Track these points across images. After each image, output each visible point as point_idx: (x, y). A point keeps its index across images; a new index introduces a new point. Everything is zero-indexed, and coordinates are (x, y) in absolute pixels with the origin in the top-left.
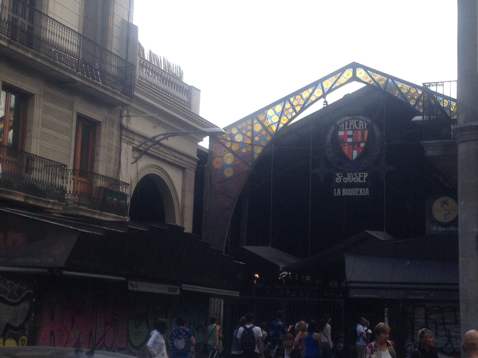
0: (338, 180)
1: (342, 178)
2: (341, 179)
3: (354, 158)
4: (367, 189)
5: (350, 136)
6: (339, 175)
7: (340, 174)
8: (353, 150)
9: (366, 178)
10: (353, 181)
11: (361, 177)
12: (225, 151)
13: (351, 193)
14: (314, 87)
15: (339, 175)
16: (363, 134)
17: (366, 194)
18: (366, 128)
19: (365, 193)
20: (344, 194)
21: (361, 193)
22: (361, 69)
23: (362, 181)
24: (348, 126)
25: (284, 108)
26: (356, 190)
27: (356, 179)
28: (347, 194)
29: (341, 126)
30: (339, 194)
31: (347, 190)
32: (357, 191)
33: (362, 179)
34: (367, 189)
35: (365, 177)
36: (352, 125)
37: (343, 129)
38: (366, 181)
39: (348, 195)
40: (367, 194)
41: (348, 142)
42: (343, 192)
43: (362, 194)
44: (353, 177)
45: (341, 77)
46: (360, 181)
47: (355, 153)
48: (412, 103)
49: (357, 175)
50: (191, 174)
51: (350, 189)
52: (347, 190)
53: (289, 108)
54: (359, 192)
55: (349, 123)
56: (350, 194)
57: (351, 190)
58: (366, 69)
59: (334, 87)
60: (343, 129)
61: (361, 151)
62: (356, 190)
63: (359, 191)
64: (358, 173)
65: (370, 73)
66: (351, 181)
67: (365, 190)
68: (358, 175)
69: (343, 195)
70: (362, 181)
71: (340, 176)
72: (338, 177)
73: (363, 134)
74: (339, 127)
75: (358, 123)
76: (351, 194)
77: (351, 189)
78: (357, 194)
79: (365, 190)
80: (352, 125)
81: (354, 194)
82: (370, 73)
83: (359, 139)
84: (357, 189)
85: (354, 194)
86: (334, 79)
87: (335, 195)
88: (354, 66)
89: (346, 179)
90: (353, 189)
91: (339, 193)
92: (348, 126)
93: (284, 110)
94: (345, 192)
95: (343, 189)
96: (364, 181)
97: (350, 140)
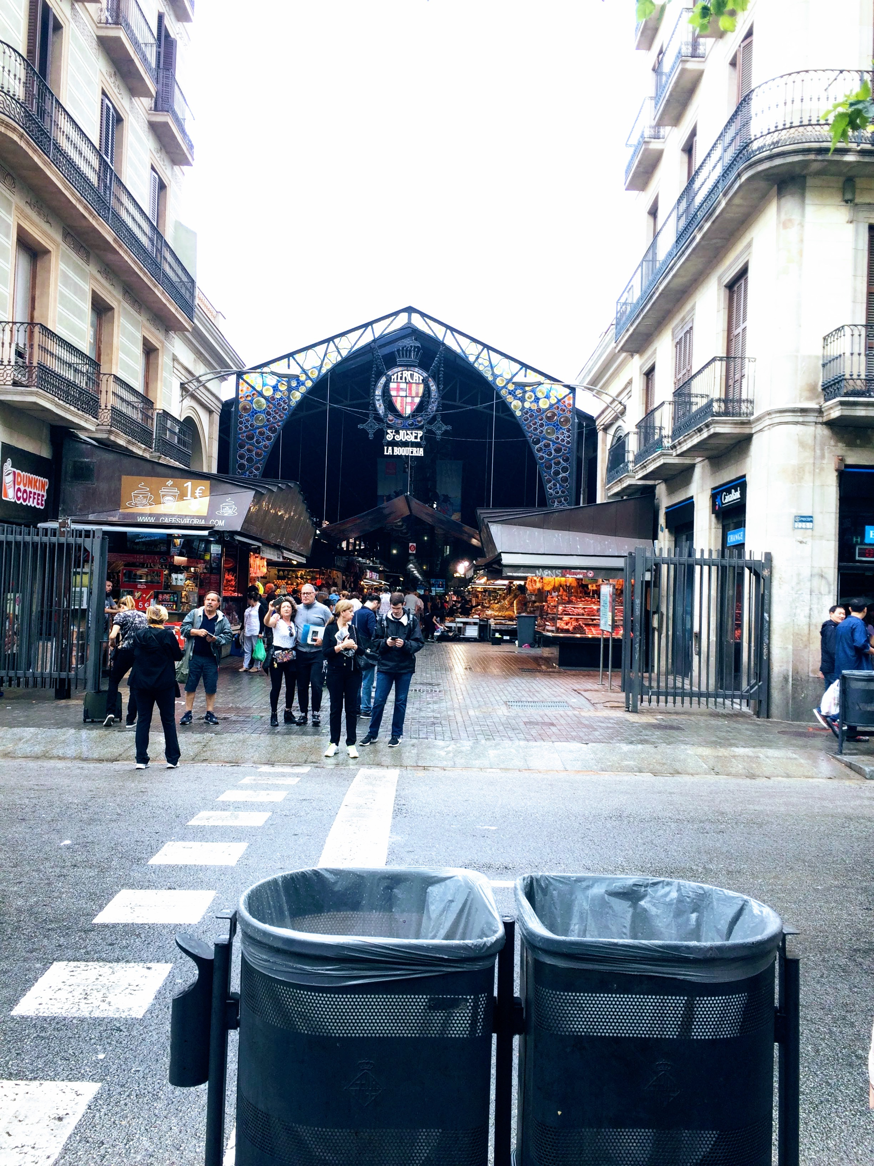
0: (389, 437)
1: (394, 436)
4: (422, 449)
14: (364, 329)
16: (417, 389)
18: (421, 381)
24: (401, 379)
29: (393, 377)
33: (416, 437)
34: (422, 449)
35: (419, 436)
36: (405, 378)
37: (395, 380)
42: (395, 451)
46: (414, 440)
48: (472, 359)
50: (216, 418)
54: (412, 452)
55: (402, 374)
58: (423, 315)
59: (385, 333)
60: (395, 380)
68: (412, 433)
70: (416, 440)
73: (417, 389)
74: (391, 378)
75: (412, 376)
78: (410, 455)
80: (405, 378)
83: (414, 394)
87: (385, 453)
88: (410, 310)
89: (397, 436)
91: (390, 452)
92: (401, 379)
96: (419, 440)
97: (403, 394)
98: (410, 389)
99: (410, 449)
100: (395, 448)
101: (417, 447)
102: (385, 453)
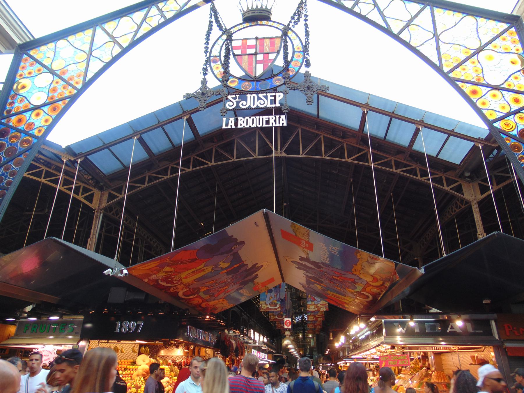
1: (238, 103)
2: (235, 104)
3: (258, 74)
4: (283, 117)
5: (250, 47)
6: (232, 98)
7: (234, 96)
8: (256, 63)
9: (279, 101)
12: (39, 70)
15: (232, 98)
16: (272, 44)
17: (281, 125)
19: (279, 123)
20: (241, 125)
25: (147, 15)
26: (263, 119)
27: (262, 102)
28: (247, 125)
30: (231, 126)
31: (247, 120)
34: (283, 117)
38: (280, 106)
39: (246, 126)
40: (283, 124)
43: (274, 125)
44: (258, 100)
46: (269, 105)
49: (263, 96)
51: (252, 118)
52: (247, 120)
54: (268, 122)
56: (252, 126)
57: (253, 119)
62: (263, 119)
63: (268, 119)
64: (266, 93)
66: (254, 105)
67: (280, 118)
68: (266, 97)
69: (239, 126)
70: (273, 106)
71: (235, 98)
72: (231, 101)
76: (254, 126)
78: (265, 125)
79: (280, 118)
81: (259, 124)
84: (264, 117)
85: (259, 124)
89: (245, 103)
90: (258, 117)
93: (148, 17)
94: (244, 122)
95: (239, 118)
98: (262, 45)
99: (265, 118)
101: (276, 114)
102: (224, 127)
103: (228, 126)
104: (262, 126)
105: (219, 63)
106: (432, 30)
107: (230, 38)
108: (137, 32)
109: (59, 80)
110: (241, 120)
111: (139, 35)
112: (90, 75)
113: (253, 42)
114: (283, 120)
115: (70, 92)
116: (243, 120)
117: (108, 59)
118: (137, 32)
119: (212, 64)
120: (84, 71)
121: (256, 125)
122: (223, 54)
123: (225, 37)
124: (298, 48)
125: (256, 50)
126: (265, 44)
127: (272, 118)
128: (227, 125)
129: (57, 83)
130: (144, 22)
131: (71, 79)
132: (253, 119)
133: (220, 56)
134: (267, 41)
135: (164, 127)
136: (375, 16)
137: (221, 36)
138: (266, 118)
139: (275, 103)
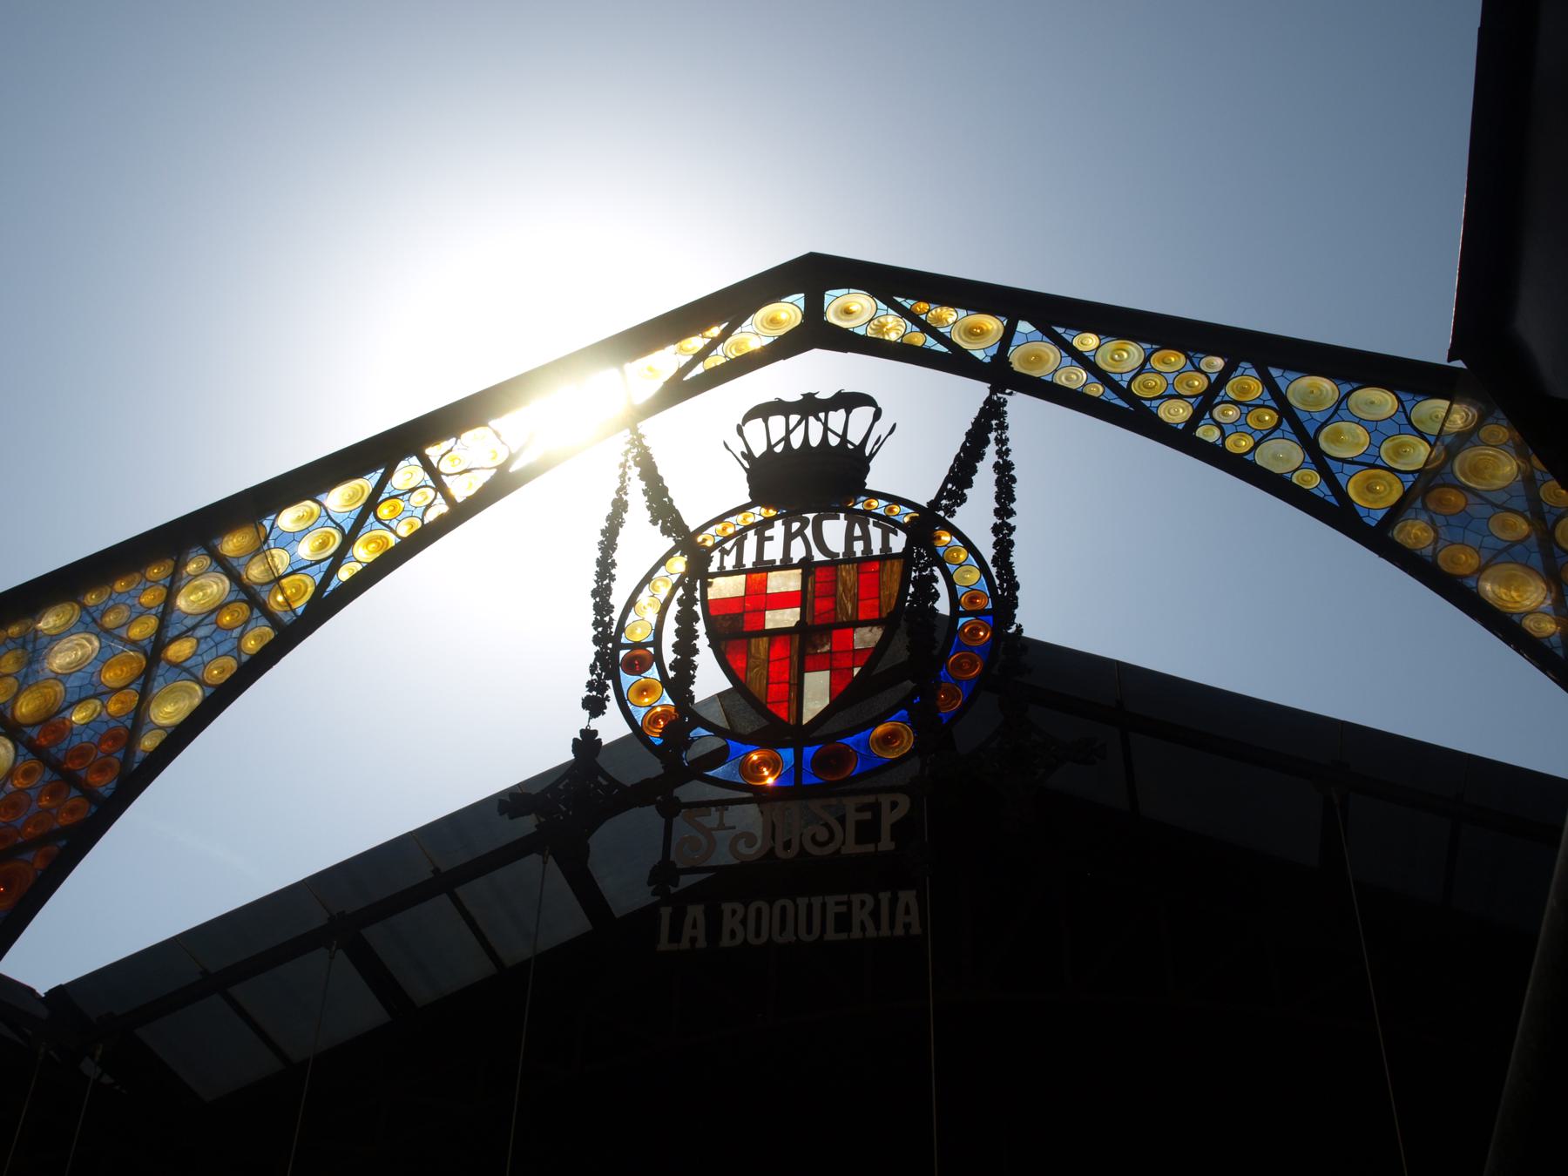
5: (782, 601)
9: (894, 826)
10: (803, 851)
11: (859, 824)
13: (783, 928)
17: (899, 931)
19: (892, 926)
20: (733, 934)
21: (862, 923)
22: (852, 291)
23: (870, 848)
26: (824, 905)
27: (823, 835)
28: (758, 934)
30: (693, 940)
31: (759, 911)
32: (832, 910)
33: (867, 831)
34: (907, 897)
35: (888, 818)
40: (907, 926)
41: (769, 625)
42: (729, 923)
43: (871, 932)
45: (739, 330)
46: (851, 848)
47: (817, 692)
52: (759, 911)
53: (412, 490)
54: (843, 922)
57: (784, 909)
61: (856, 671)
62: (824, 905)
63: (843, 909)
65: (908, 303)
67: (894, 901)
69: (726, 942)
70: (870, 848)
76: (789, 936)
77: (788, 903)
78: (831, 935)
79: (894, 901)
81: (809, 931)
82: (904, 304)
85: (809, 931)
86: (696, 343)
87: (664, 945)
90: (802, 902)
94: (744, 922)
95: (727, 907)
96: (886, 844)
100: (727, 907)
103: (678, 941)
104: (821, 937)
105: (653, 673)
106: (1520, 503)
107: (699, 571)
108: (339, 558)
109: (35, 764)
110: (734, 912)
111: (344, 574)
112: (149, 742)
113: (789, 582)
114: (907, 912)
115: (72, 811)
116: (740, 915)
117: (217, 672)
118: (339, 558)
119: (627, 680)
120: (129, 723)
121: (796, 933)
122: (669, 637)
123: (679, 564)
124: (972, 600)
125: (803, 614)
126: (840, 588)
127: (863, 904)
128: (675, 936)
129: (28, 774)
130: (371, 518)
131: (81, 753)
132: (784, 909)
133: (657, 641)
134: (848, 574)
135: (460, 891)
136: (1282, 455)
137: (663, 561)
138: (837, 904)
139: (876, 839)
